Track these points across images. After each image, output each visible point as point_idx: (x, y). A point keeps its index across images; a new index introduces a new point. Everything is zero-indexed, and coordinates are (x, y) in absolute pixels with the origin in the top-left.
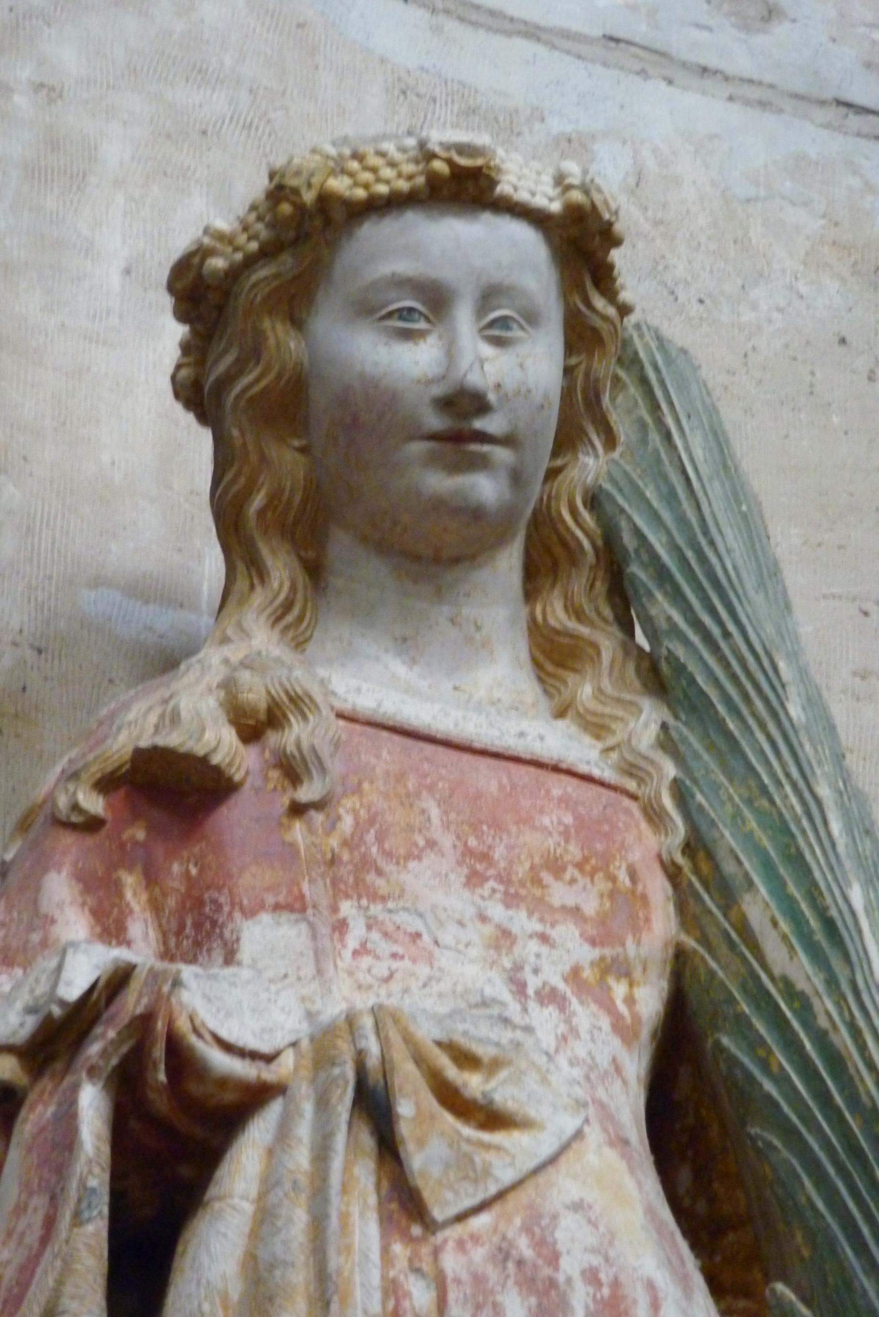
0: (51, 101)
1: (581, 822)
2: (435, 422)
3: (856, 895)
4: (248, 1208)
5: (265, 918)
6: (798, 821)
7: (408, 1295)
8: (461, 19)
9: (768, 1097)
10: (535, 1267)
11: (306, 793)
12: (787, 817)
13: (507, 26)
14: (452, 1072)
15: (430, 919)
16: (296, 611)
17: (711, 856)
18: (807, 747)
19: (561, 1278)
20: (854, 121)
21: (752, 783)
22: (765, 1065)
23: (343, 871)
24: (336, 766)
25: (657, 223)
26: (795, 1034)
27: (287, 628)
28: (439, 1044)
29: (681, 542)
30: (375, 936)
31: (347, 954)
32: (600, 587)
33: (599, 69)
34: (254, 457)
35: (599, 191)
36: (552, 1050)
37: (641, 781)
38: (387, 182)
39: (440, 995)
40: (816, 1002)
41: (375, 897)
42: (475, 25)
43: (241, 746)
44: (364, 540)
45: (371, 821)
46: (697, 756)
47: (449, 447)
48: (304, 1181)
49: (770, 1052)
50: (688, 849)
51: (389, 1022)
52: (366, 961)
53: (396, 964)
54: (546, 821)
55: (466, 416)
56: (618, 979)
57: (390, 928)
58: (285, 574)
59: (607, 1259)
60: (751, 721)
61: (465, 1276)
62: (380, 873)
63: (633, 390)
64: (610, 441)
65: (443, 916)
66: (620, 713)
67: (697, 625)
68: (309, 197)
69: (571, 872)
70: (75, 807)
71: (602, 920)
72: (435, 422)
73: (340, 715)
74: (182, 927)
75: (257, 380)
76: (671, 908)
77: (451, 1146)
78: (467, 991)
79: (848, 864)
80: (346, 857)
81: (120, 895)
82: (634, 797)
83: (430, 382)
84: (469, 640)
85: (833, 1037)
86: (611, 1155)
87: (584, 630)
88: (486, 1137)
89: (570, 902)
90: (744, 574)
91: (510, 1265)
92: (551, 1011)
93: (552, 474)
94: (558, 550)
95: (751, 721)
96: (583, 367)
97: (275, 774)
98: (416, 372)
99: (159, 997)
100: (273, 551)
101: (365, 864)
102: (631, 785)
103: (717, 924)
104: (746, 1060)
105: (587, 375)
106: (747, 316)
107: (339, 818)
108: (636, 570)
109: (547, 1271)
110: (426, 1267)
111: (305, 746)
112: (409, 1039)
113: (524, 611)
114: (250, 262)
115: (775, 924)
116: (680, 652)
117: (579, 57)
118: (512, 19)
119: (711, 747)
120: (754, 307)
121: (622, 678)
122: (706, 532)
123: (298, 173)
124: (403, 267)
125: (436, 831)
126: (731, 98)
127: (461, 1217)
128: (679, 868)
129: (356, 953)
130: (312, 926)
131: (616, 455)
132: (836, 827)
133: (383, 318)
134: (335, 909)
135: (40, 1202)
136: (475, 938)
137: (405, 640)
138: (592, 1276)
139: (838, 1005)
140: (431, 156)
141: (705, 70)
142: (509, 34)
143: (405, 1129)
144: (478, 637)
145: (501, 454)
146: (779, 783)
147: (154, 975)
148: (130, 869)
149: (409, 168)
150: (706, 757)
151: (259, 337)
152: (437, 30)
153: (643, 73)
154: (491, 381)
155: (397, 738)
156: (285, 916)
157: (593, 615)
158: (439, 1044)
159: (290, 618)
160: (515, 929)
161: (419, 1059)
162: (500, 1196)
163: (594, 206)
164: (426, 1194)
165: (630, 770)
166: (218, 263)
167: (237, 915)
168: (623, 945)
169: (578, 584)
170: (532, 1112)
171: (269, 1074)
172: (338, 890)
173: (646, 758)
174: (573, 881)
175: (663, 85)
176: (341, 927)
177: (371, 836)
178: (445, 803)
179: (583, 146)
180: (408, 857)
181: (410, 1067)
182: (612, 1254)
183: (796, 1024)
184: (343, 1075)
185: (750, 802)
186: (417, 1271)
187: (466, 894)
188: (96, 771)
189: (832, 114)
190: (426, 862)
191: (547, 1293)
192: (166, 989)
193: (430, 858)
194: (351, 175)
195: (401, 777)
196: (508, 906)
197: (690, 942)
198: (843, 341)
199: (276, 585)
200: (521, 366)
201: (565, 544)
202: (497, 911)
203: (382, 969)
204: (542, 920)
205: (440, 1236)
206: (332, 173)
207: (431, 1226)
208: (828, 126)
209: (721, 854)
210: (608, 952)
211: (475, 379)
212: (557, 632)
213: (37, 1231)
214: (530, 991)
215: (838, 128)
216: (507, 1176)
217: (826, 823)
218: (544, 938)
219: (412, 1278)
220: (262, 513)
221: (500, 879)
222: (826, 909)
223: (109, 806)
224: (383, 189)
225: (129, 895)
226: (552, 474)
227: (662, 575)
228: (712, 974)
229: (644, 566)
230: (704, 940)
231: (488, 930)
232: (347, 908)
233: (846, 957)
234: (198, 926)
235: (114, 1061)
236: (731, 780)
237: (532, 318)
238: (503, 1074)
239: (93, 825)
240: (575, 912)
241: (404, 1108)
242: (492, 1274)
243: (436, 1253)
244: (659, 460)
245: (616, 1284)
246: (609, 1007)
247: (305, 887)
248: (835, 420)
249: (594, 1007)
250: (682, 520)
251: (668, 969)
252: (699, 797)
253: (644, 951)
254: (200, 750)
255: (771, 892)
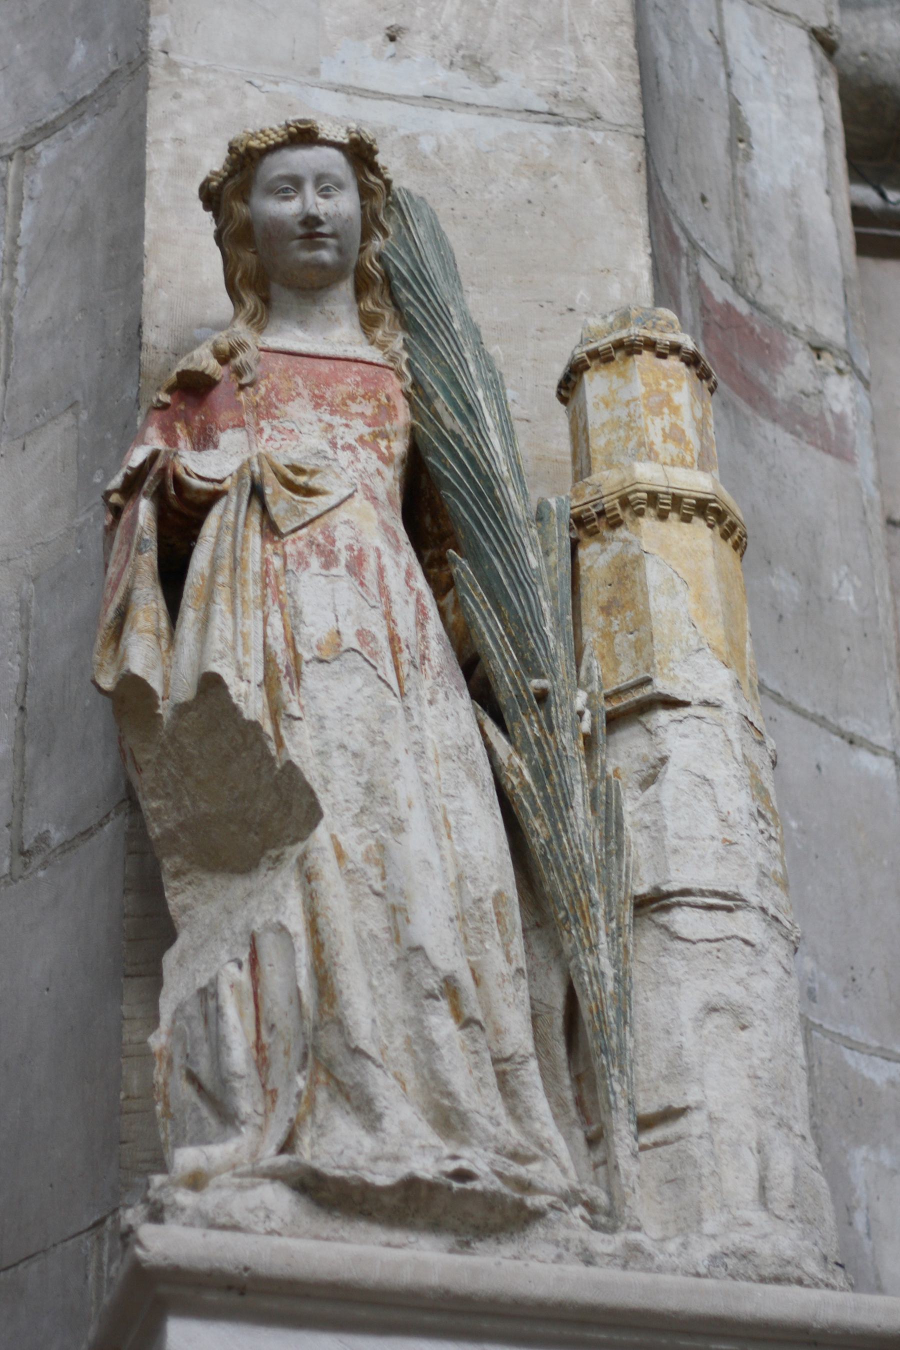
0: (180, 145)
1: (364, 380)
2: (300, 231)
3: (480, 394)
4: (212, 540)
5: (229, 431)
6: (456, 368)
7: (273, 563)
8: (360, 96)
9: (446, 478)
10: (325, 546)
11: (245, 380)
12: (452, 366)
13: (380, 96)
14: (290, 475)
15: (298, 423)
16: (258, 316)
17: (422, 387)
18: (461, 339)
19: (336, 549)
20: (534, 117)
21: (438, 356)
22: (445, 466)
23: (261, 409)
24: (257, 369)
25: (448, 164)
26: (456, 451)
27: (254, 324)
28: (287, 466)
29: (412, 268)
30: (275, 433)
31: (263, 441)
32: (386, 292)
33: (422, 109)
34: (235, 257)
35: (364, 132)
36: (345, 467)
37: (395, 362)
38: (273, 139)
39: (300, 452)
40: (463, 438)
41: (275, 417)
42: (366, 97)
43: (219, 366)
44: (283, 285)
45: (273, 389)
46: (416, 349)
47: (308, 240)
48: (231, 525)
49: (446, 460)
50: (413, 386)
51: (264, 459)
52: (271, 443)
53: (282, 443)
54: (349, 380)
55: (313, 227)
56: (382, 439)
57: (281, 429)
58: (252, 303)
59: (357, 541)
60: (438, 332)
61: (294, 553)
62: (276, 408)
63: (397, 214)
64: (385, 233)
65: (303, 422)
66: (391, 339)
67: (418, 298)
68: (242, 150)
69: (360, 399)
70: (159, 401)
71: (374, 417)
72: (300, 231)
73: (261, 350)
74: (199, 440)
75: (232, 227)
76: (408, 410)
77: (288, 503)
78: (311, 448)
79: (477, 382)
80: (262, 403)
81: (175, 431)
82: (392, 369)
83: (297, 215)
84: (329, 319)
85: (471, 450)
86: (368, 504)
87: (379, 310)
88: (305, 499)
89: (360, 411)
90: (438, 277)
91: (314, 547)
92: (348, 453)
93: (362, 250)
94: (367, 280)
95: (438, 332)
96: (368, 205)
97: (233, 375)
98: (291, 212)
99: (168, 460)
100: (247, 295)
101: (271, 405)
102: (391, 365)
103: (425, 413)
104: (438, 466)
105: (371, 208)
106: (487, 196)
107: (259, 389)
108: (396, 282)
109: (330, 547)
110: (279, 552)
111: (243, 362)
112: (273, 466)
113: (356, 307)
114: (226, 180)
115: (447, 409)
116: (412, 311)
117: (412, 105)
118: (383, 94)
119: (423, 346)
120: (490, 192)
121: (394, 325)
122: (422, 263)
123: (237, 141)
124: (282, 171)
125: (301, 390)
126: (480, 114)
127: (294, 531)
128: (410, 394)
129: (267, 440)
130: (247, 431)
131: (389, 239)
132: (472, 368)
133: (276, 193)
134: (258, 424)
135: (125, 547)
136: (317, 428)
137: (302, 322)
138: (350, 548)
139: (473, 438)
140: (288, 126)
141: (468, 105)
142: (381, 99)
143: (268, 499)
144: (333, 317)
145: (331, 241)
146: (449, 355)
147: (166, 452)
148: (179, 421)
149: (282, 132)
150: (419, 349)
151: (231, 209)
152: (350, 101)
153: (441, 109)
154: (322, 212)
155: (286, 356)
156: (237, 429)
157: (383, 304)
158: (287, 466)
159: (255, 320)
160: (334, 423)
161: (276, 472)
162: (312, 521)
163: (362, 138)
164: (278, 523)
165: (392, 359)
166: (215, 184)
167: (218, 432)
168: (384, 425)
169: (376, 294)
170: (327, 488)
171: (218, 487)
172: (260, 416)
173: (398, 354)
174: (361, 402)
175: (450, 112)
176: (261, 431)
177: (273, 395)
178: (305, 379)
179: (414, 138)
180: (289, 400)
181: (272, 475)
182: (360, 538)
183: (456, 448)
184: (246, 483)
185: (438, 364)
186: (276, 554)
187: (314, 412)
188: (166, 386)
189: (524, 115)
190: (296, 401)
191: (329, 556)
192: (171, 457)
193: (298, 400)
194: (259, 139)
195: (286, 370)
196: (331, 415)
197: (416, 423)
198: (530, 202)
199: (248, 307)
200: (336, 205)
201: (370, 277)
202: (327, 417)
203: (277, 445)
204: (346, 419)
205: (285, 539)
206: (251, 139)
207: (281, 536)
208: (522, 120)
209: (426, 385)
210: (377, 429)
211: (313, 211)
212: (368, 312)
213: (125, 558)
214: (339, 446)
215: (526, 121)
216: (314, 513)
217: (468, 367)
218: (347, 426)
219: (274, 557)
220: (240, 280)
221: (328, 405)
222: (468, 400)
223: (172, 398)
224: (272, 142)
225: (178, 431)
226: (362, 250)
227: (405, 282)
228: (424, 433)
229: (398, 280)
230: (422, 422)
231: (322, 425)
232: (263, 423)
233: (476, 419)
234: (205, 439)
235: (154, 489)
236: (430, 357)
237: (340, 186)
238: (318, 476)
239: (165, 406)
240: (362, 415)
241: (268, 491)
242: (306, 551)
243: (283, 546)
244: (405, 238)
245: (361, 550)
246: (378, 451)
247: (245, 417)
248: (527, 232)
249: (369, 450)
250: (414, 260)
251: (408, 435)
252: (417, 365)
253: (395, 428)
254: (200, 369)
255: (445, 397)
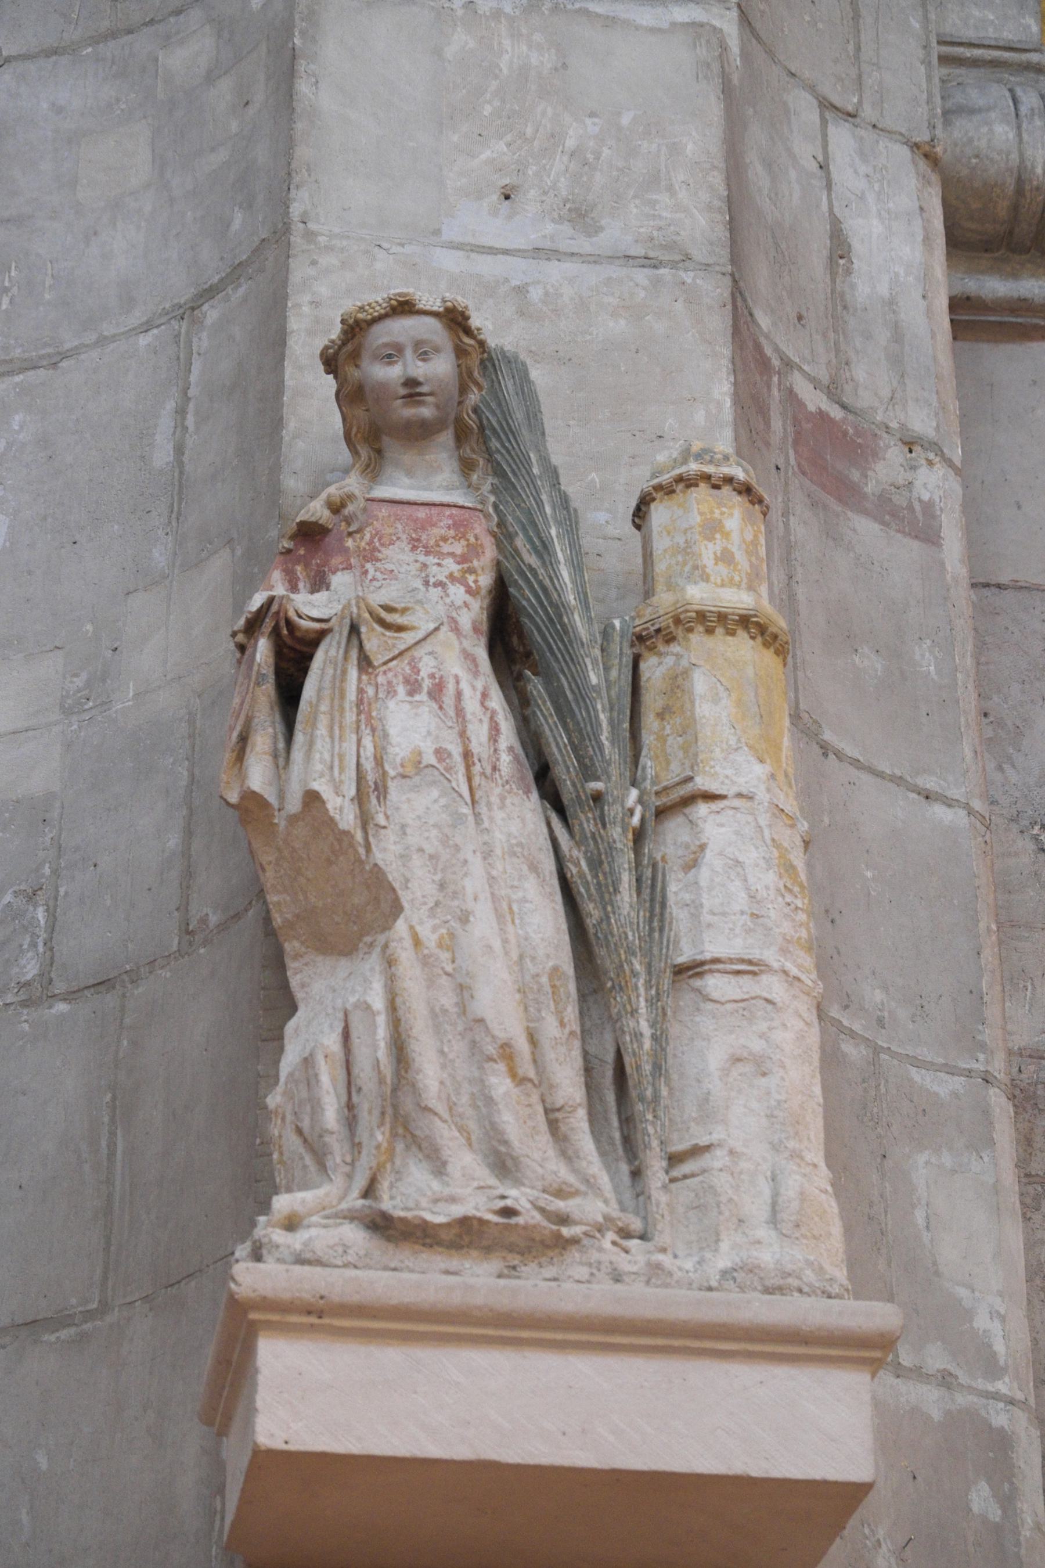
3: (553, 532)
5: (339, 573)
7: (366, 692)
9: (524, 607)
14: (383, 614)
16: (372, 466)
17: (505, 527)
24: (362, 518)
31: (367, 581)
41: (378, 560)
45: (376, 534)
50: (499, 525)
61: (385, 683)
62: (379, 551)
67: (504, 446)
68: (351, 321)
70: (283, 547)
72: (403, 391)
82: (481, 511)
86: (452, 636)
87: (474, 456)
88: (396, 635)
93: (460, 403)
101: (375, 549)
108: (487, 432)
114: (340, 348)
124: (385, 339)
131: (483, 393)
134: (363, 567)
143: (363, 636)
153: (548, 259)
156: (345, 572)
166: (331, 351)
170: (415, 624)
171: (324, 626)
177: (376, 540)
183: (532, 580)
193: (398, 543)
197: (501, 558)
202: (422, 558)
206: (359, 312)
209: (508, 524)
210: (465, 566)
216: (402, 647)
218: (439, 565)
220: (356, 435)
221: (424, 547)
226: (460, 403)
227: (494, 430)
230: (506, 557)
231: (418, 565)
237: (437, 350)
240: (452, 554)
245: (441, 677)
252: (501, 507)
254: (313, 519)
